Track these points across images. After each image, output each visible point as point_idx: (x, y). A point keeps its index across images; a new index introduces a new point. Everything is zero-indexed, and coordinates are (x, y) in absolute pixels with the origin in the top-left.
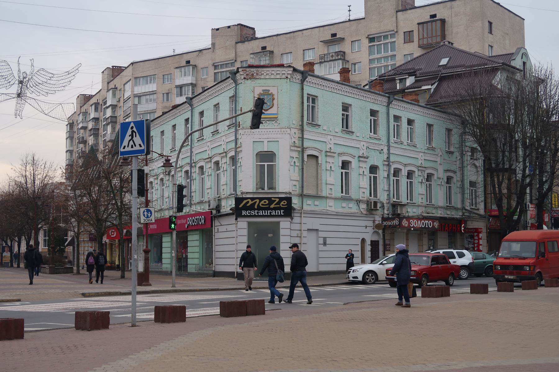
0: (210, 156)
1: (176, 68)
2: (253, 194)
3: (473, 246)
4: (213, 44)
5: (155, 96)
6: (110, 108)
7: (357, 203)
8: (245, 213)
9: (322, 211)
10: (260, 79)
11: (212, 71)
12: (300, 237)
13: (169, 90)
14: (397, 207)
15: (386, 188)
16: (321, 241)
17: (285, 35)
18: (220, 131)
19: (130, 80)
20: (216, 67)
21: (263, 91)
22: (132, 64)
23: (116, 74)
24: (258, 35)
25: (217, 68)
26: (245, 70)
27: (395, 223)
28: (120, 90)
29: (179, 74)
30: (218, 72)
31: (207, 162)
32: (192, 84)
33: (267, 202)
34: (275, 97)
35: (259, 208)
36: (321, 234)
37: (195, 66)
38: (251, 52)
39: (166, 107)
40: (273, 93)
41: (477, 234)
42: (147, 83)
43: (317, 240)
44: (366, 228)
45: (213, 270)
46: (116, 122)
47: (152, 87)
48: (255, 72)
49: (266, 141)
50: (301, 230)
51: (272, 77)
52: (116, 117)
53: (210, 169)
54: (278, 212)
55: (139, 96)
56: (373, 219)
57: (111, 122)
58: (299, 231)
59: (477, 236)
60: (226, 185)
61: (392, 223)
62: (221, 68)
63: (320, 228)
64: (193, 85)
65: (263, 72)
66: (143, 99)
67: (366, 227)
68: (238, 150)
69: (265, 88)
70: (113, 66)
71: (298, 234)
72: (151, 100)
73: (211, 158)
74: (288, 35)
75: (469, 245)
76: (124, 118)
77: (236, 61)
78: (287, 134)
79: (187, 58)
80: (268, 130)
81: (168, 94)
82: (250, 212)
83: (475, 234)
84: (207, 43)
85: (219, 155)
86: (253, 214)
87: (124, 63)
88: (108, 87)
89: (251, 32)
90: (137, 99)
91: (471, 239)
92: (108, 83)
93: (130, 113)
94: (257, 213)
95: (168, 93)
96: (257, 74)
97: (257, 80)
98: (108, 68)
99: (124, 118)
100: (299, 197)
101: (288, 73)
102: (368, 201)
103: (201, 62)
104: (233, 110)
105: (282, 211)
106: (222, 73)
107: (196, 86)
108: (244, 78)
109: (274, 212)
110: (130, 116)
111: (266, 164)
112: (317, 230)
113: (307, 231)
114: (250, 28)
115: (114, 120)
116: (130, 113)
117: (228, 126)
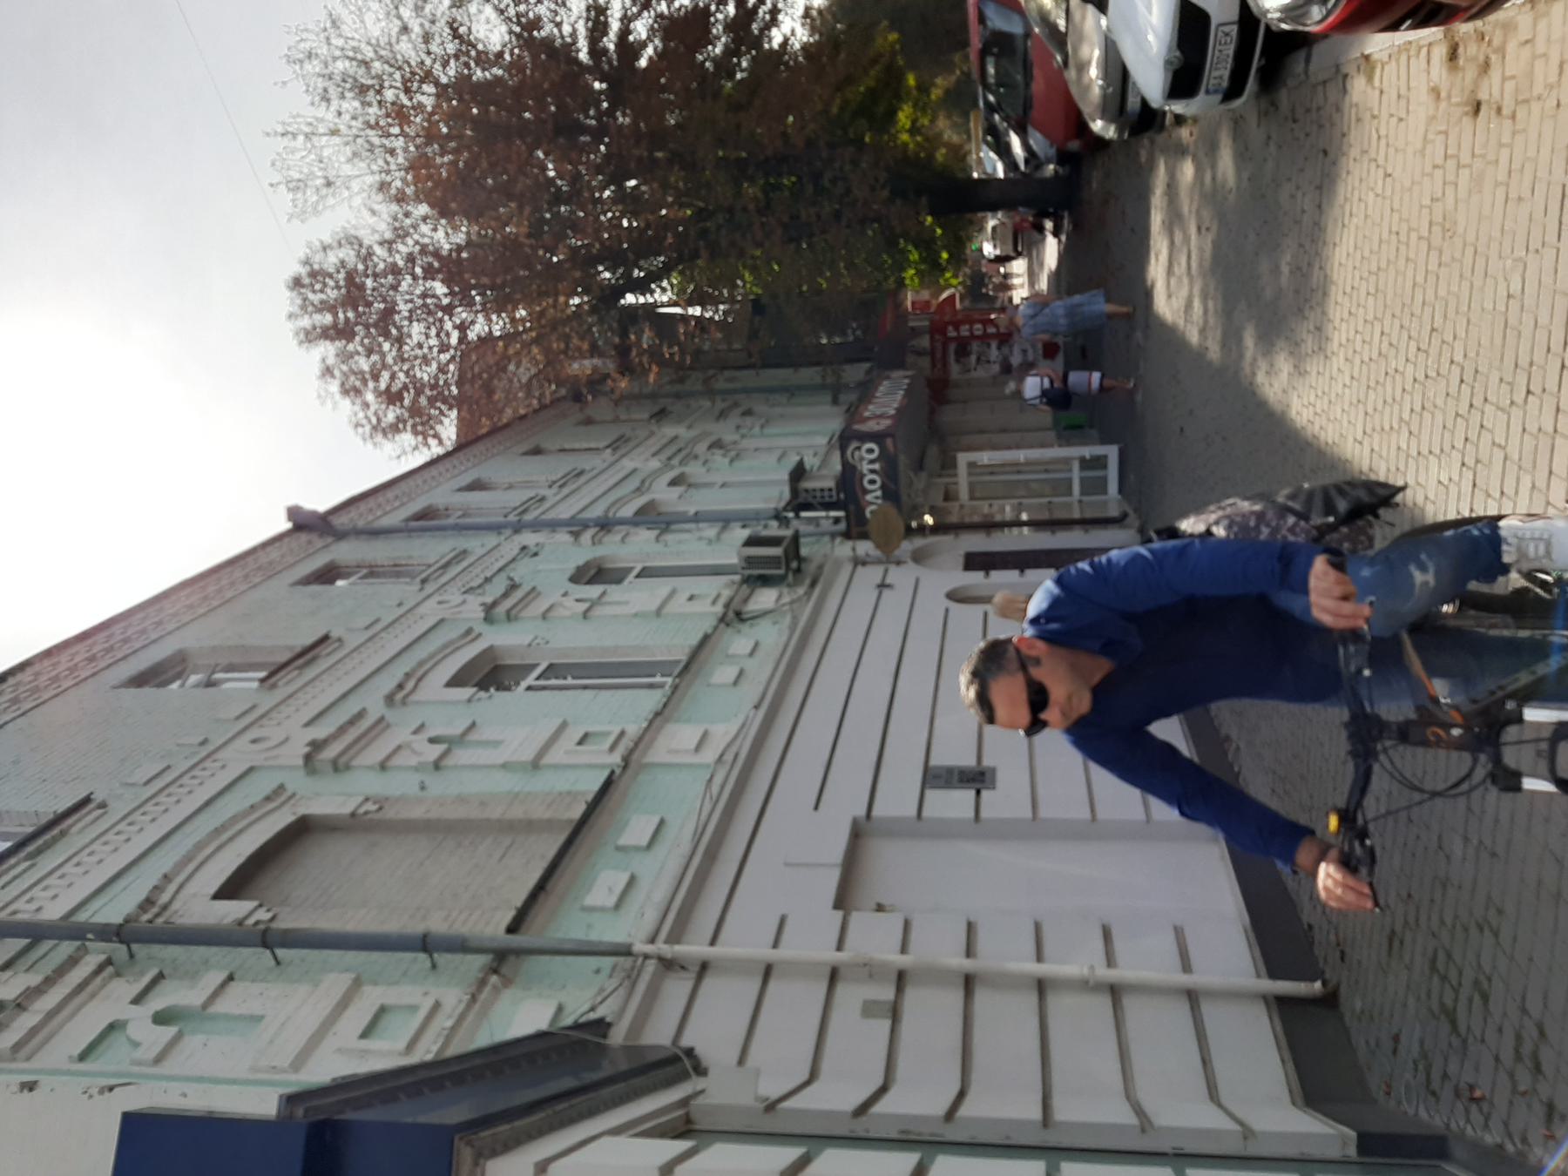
3: (994, 345)
7: (742, 620)
9: (715, 789)
12: (901, 979)
14: (807, 491)
15: (711, 531)
16: (954, 803)
27: (872, 462)
36: (897, 799)
41: (950, 328)
43: (945, 831)
44: (889, 586)
50: (834, 975)
56: (848, 568)
58: (840, 989)
59: (957, 329)
61: (872, 482)
63: (847, 802)
67: (883, 586)
71: (869, 1009)
75: (993, 358)
83: (952, 333)
91: (968, 354)
100: (507, 982)
102: (747, 580)
112: (858, 834)
113: (856, 918)
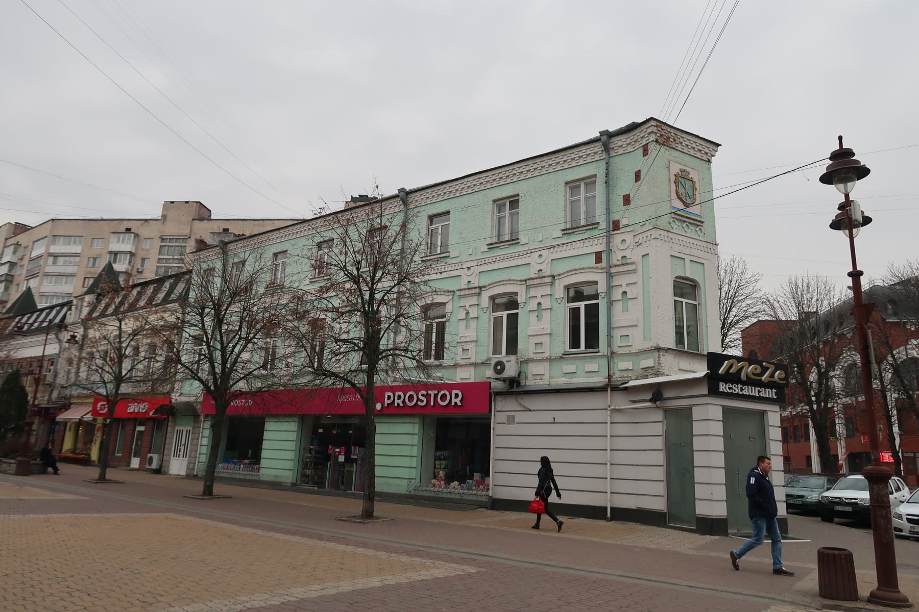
0: (476, 285)
1: (113, 233)
2: (675, 352)
4: (164, 217)
5: (77, 259)
6: (8, 265)
8: (724, 387)
10: (677, 150)
11: (157, 243)
13: (98, 255)
17: (252, 221)
18: (523, 239)
19: (46, 237)
20: (163, 239)
21: (681, 171)
22: (53, 220)
23: (18, 231)
24: (213, 217)
25: (164, 241)
26: (660, 126)
28: (25, 248)
29: (116, 239)
30: (165, 246)
31: (460, 297)
32: (130, 252)
33: (759, 370)
34: (697, 185)
35: (750, 382)
37: (137, 235)
38: (210, 232)
39: (90, 273)
40: (694, 180)
42: (69, 243)
45: (490, 495)
46: (11, 282)
47: (76, 249)
48: (672, 134)
49: (688, 259)
51: (692, 152)
52: (13, 276)
53: (475, 309)
54: (769, 391)
55: (56, 256)
57: (6, 280)
60: (549, 335)
62: (169, 242)
64: (132, 254)
65: (681, 140)
66: (61, 260)
68: (613, 270)
69: (684, 168)
70: (16, 223)
72: (70, 263)
73: (480, 288)
74: (257, 222)
76: (26, 277)
77: (189, 237)
78: (713, 255)
79: (128, 225)
80: (692, 241)
81: (95, 259)
82: (731, 386)
84: (157, 213)
85: (520, 283)
86: (735, 390)
87: (30, 220)
88: (5, 243)
89: (208, 213)
90: (51, 259)
92: (6, 239)
93: (38, 273)
94: (742, 390)
95: (96, 258)
96: (675, 140)
97: (672, 150)
98: (9, 223)
99: (27, 278)
101: (712, 153)
103: (144, 232)
104: (428, 235)
105: (774, 391)
106: (170, 248)
107: (134, 256)
108: (657, 141)
109: (764, 392)
110: (38, 276)
111: (684, 301)
114: (207, 209)
115: (9, 278)
116: (38, 273)
117: (563, 230)
